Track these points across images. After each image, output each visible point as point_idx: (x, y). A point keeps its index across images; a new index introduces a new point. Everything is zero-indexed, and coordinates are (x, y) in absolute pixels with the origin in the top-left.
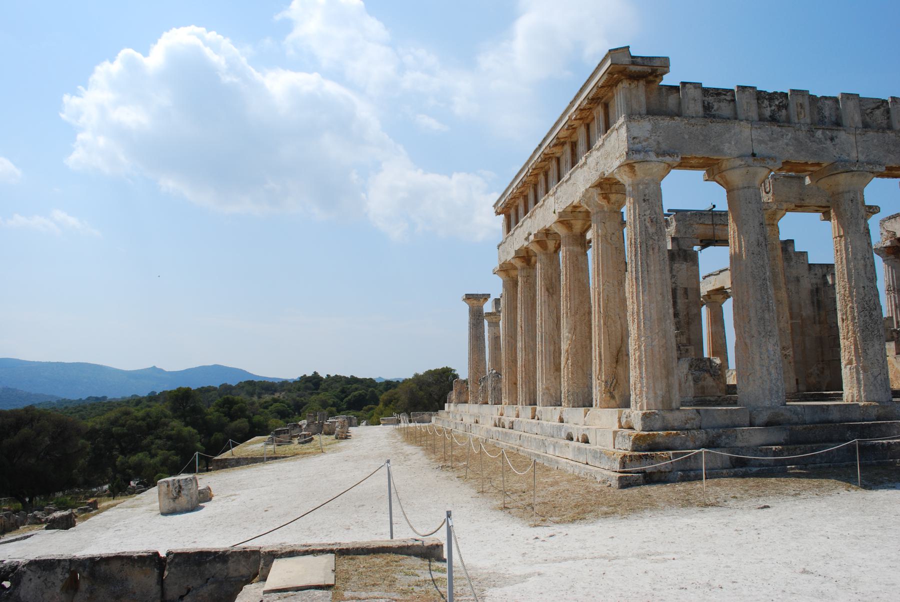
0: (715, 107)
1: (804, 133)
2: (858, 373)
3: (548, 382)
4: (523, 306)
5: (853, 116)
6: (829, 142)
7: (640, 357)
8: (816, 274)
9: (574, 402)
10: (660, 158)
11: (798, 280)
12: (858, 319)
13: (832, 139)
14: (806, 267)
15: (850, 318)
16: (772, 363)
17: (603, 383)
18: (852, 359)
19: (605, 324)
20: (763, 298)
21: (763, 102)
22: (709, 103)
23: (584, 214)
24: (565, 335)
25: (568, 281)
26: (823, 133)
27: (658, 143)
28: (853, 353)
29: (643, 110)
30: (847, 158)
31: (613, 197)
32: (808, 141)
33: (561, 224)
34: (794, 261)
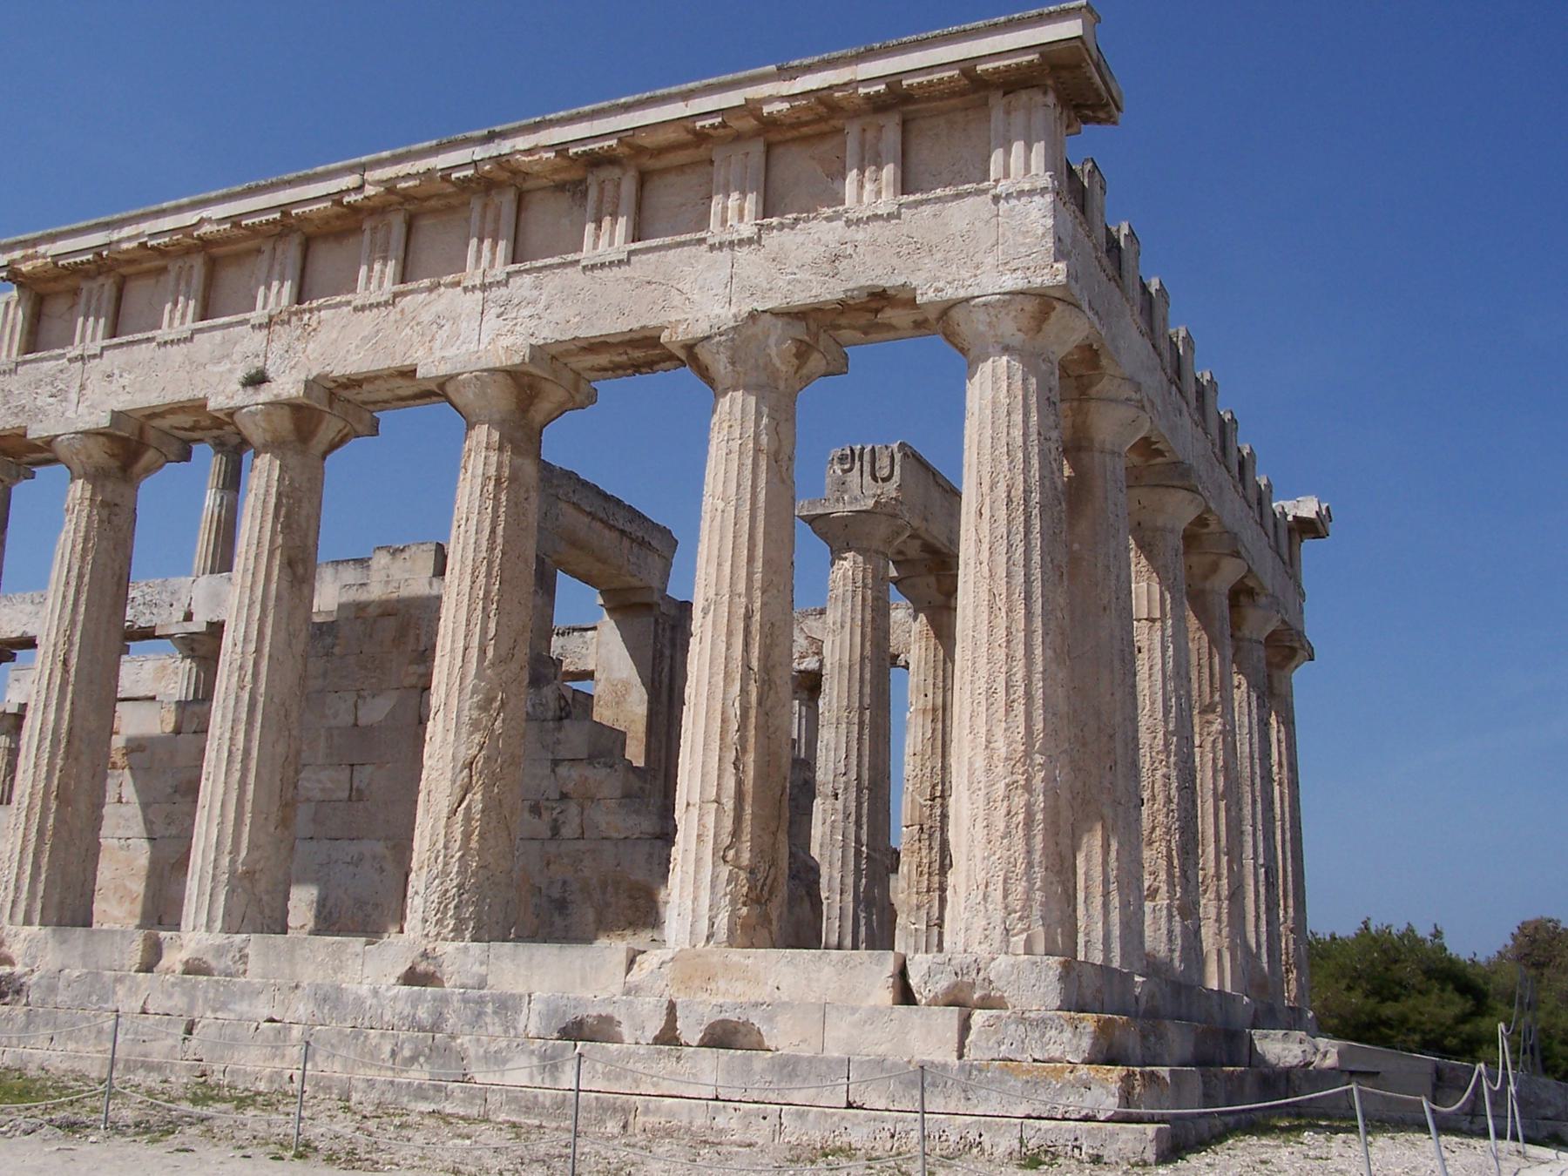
2: (1170, 917)
3: (257, 855)
4: (83, 598)
7: (1029, 807)
9: (477, 928)
12: (1178, 804)
15: (1161, 798)
17: (743, 875)
18: (1159, 888)
19: (760, 703)
23: (572, 376)
24: (466, 712)
25: (498, 552)
28: (1163, 876)
31: (816, 362)
33: (509, 381)
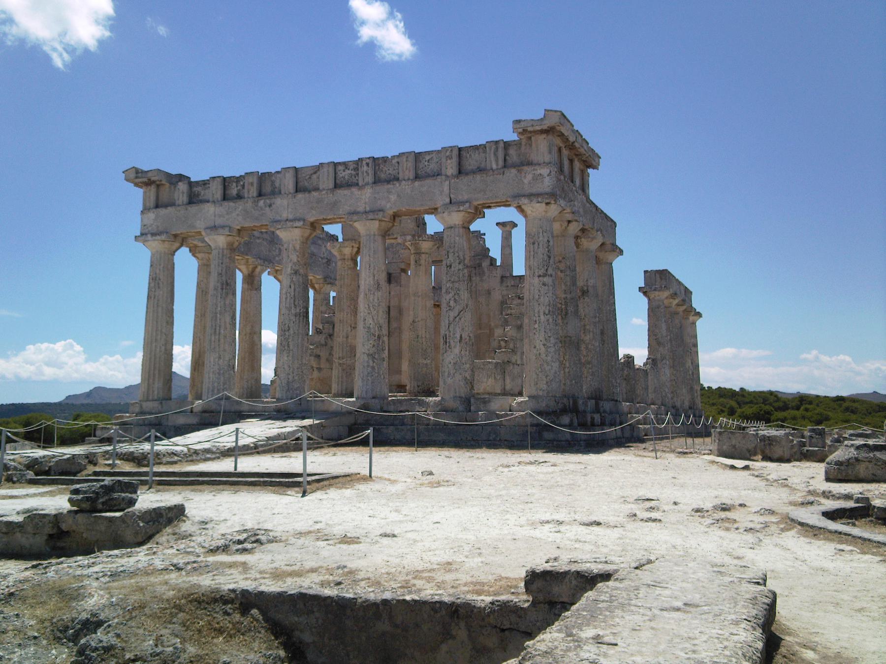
0: (202, 194)
1: (251, 204)
5: (289, 183)
6: (267, 208)
8: (508, 286)
10: (154, 238)
11: (489, 292)
13: (270, 206)
14: (498, 279)
16: (212, 370)
20: (212, 325)
21: (232, 185)
22: (198, 192)
26: (264, 203)
27: (158, 227)
29: (152, 204)
30: (279, 218)
32: (253, 210)
34: (487, 274)
